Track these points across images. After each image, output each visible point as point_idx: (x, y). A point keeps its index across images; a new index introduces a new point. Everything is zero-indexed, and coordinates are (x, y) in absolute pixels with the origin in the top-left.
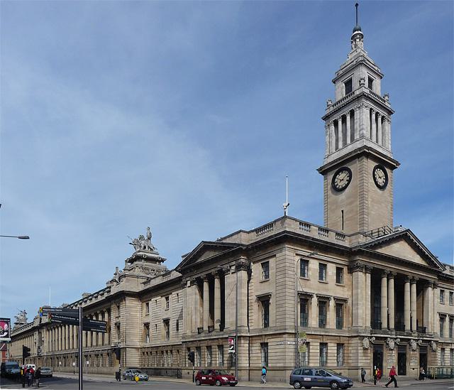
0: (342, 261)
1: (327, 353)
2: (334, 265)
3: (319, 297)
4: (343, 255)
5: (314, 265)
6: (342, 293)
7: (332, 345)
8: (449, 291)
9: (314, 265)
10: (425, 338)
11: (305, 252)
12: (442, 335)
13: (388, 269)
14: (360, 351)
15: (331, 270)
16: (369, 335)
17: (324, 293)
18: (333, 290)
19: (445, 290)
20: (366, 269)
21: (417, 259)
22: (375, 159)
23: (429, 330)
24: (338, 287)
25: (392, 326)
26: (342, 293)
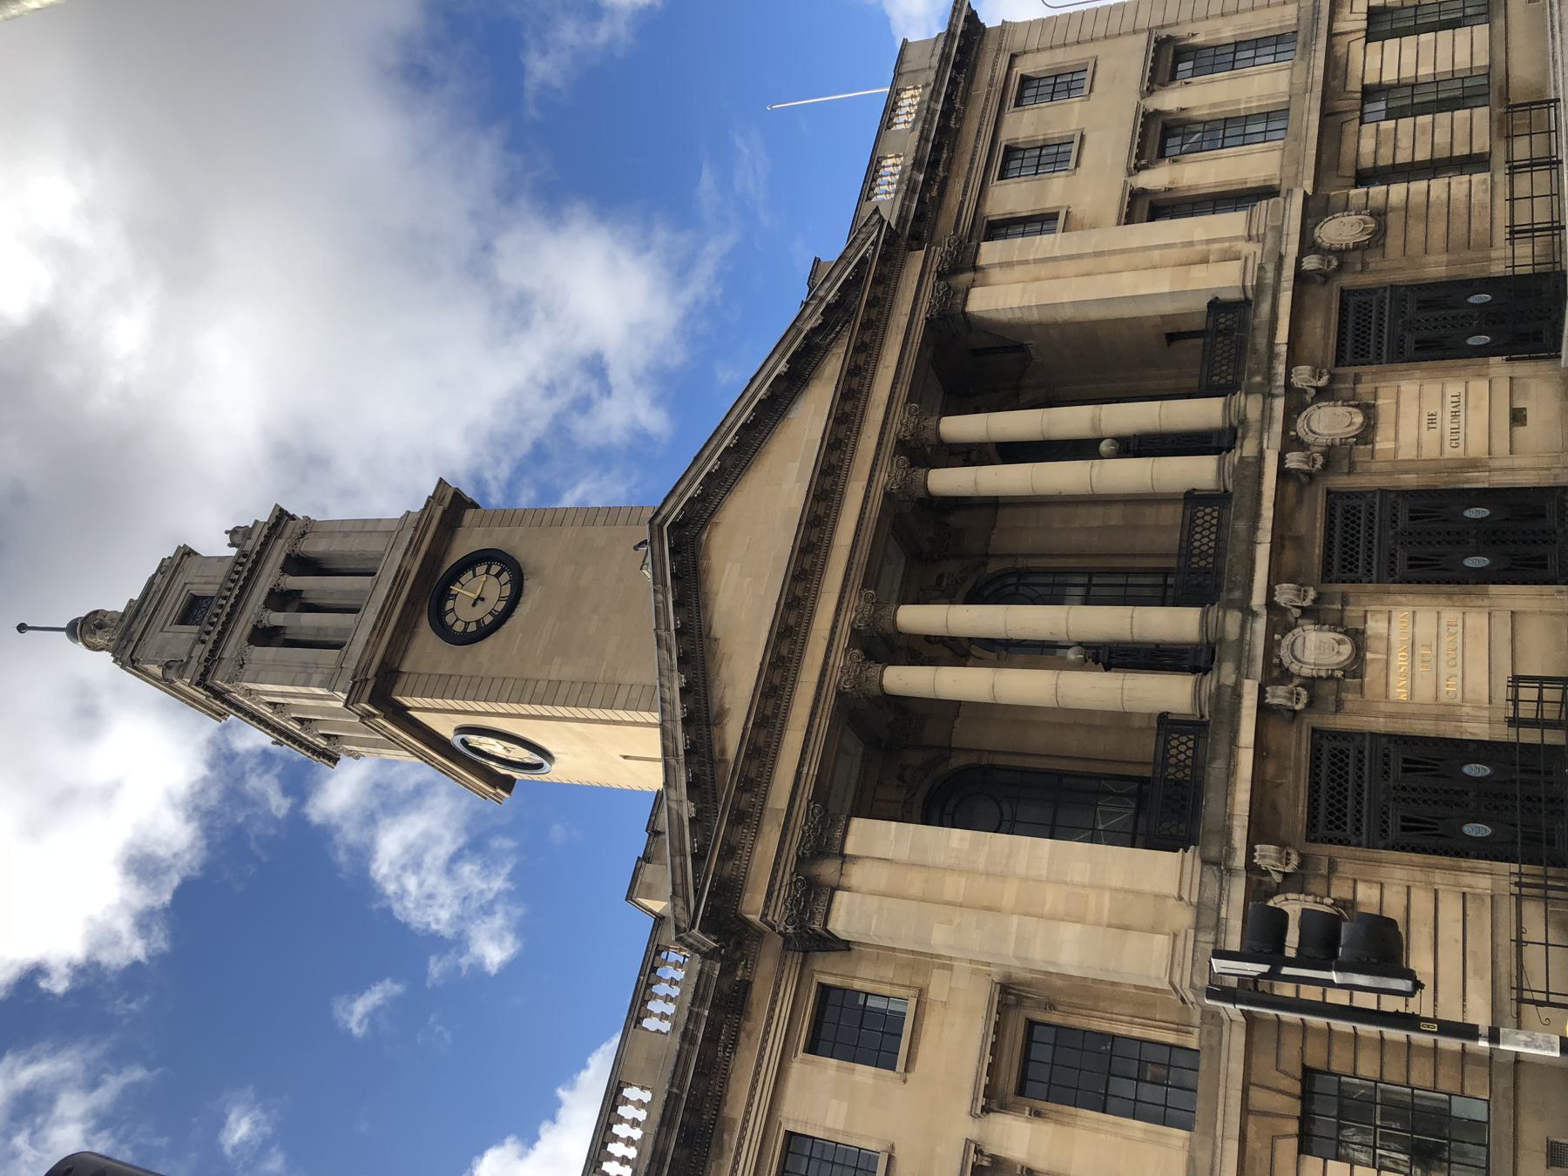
4: (746, 986)
10: (1283, 349)
12: (1272, 119)
13: (838, 660)
19: (1006, 136)
22: (405, 630)
23: (1225, 279)
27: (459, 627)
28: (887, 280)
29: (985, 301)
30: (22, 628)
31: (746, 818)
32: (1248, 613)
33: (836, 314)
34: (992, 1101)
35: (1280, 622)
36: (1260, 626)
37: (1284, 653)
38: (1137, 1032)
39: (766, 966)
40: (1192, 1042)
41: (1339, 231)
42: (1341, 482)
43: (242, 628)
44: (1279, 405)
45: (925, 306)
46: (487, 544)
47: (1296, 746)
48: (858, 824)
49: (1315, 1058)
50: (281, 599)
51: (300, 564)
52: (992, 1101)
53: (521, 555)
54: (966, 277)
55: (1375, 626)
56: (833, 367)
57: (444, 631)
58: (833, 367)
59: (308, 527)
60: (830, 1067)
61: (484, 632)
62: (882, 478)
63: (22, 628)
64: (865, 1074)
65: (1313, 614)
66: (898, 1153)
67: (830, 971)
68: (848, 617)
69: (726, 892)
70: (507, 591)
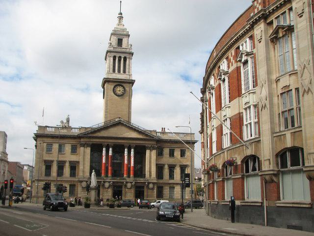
0: (73, 142)
2: (70, 145)
5: (56, 147)
6: (75, 158)
8: (179, 149)
9: (56, 147)
11: (50, 140)
13: (106, 144)
15: (68, 148)
16: (86, 180)
17: (61, 158)
20: (83, 145)
21: (134, 135)
26: (74, 158)
28: (151, 140)
29: (148, 152)
30: (121, 2)
31: (90, 137)
33: (147, 135)
34: (70, 162)
35: (109, 182)
39: (78, 140)
41: (151, 186)
43: (115, 54)
50: (120, 57)
51: (125, 59)
53: (125, 95)
57: (115, 87)
59: (130, 59)
60: (70, 148)
63: (121, 2)
64: (70, 151)
65: (110, 185)
67: (78, 146)
68: (110, 143)
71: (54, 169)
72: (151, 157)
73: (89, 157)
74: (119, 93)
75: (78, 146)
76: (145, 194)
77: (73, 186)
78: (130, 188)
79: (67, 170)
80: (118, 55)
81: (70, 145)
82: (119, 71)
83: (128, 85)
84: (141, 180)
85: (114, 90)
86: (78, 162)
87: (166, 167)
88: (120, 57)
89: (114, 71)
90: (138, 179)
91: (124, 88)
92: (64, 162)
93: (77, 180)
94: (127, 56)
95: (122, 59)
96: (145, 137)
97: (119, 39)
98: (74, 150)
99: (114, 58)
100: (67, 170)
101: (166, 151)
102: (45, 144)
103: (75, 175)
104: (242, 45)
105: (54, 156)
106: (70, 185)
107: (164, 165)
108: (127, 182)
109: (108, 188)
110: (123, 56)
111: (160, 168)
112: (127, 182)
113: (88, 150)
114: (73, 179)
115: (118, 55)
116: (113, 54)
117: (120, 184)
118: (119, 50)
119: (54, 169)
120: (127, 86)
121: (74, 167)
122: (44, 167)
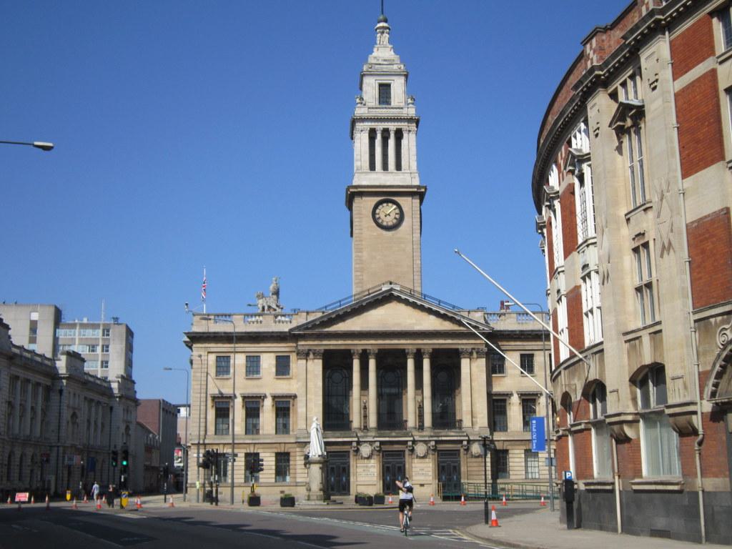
0: (282, 347)
1: (233, 465)
3: (244, 398)
5: (239, 361)
7: (268, 454)
9: (239, 361)
10: (440, 439)
13: (360, 348)
14: (299, 463)
15: (268, 362)
17: (252, 388)
18: (269, 384)
19: (535, 353)
20: (305, 355)
24: (279, 381)
25: (373, 421)
26: (283, 387)
27: (377, 211)
29: (465, 363)
32: (374, 437)
34: (274, 397)
35: (371, 443)
36: (371, 439)
37: (366, 444)
38: (291, 422)
40: (291, 433)
42: (407, 453)
43: (373, 125)
44: (427, 439)
45: (463, 347)
46: (405, 209)
47: (346, 448)
48: (320, 361)
49: (291, 454)
50: (386, 132)
51: (399, 134)
52: (274, 397)
54: (475, 355)
55: (372, 461)
56: (447, 326)
57: (376, 207)
58: (447, 326)
60: (274, 362)
61: (375, 220)
62: (410, 347)
66: (260, 380)
67: (293, 357)
69: (303, 337)
70: (390, 224)
71: (238, 413)
72: (472, 372)
73: (320, 383)
74: (389, 221)
75: (293, 357)
76: (463, 469)
77: (283, 461)
78: (424, 457)
79: (267, 417)
80: (380, 126)
81: (273, 356)
82: (385, 167)
83: (410, 199)
84: (451, 435)
85: (374, 213)
86: (295, 397)
87: (515, 400)
88: (386, 132)
89: (372, 167)
90: (443, 432)
91: (399, 206)
92: (262, 398)
93: (293, 441)
94: (403, 125)
95: (392, 135)
96: (455, 328)
97: (381, 85)
98: (283, 367)
99: (372, 134)
100: (267, 417)
101: (512, 360)
102: (212, 358)
103: (289, 431)
104: (624, 84)
105: (239, 385)
106: (278, 455)
107: (509, 395)
108: (414, 442)
109: (369, 458)
110: (392, 126)
111: (497, 405)
112: (414, 442)
113: (316, 366)
114: (282, 438)
115: (380, 126)
116: (368, 125)
117: (396, 447)
118: (384, 112)
119: (238, 413)
120: (406, 202)
121: (283, 407)
122: (211, 414)
